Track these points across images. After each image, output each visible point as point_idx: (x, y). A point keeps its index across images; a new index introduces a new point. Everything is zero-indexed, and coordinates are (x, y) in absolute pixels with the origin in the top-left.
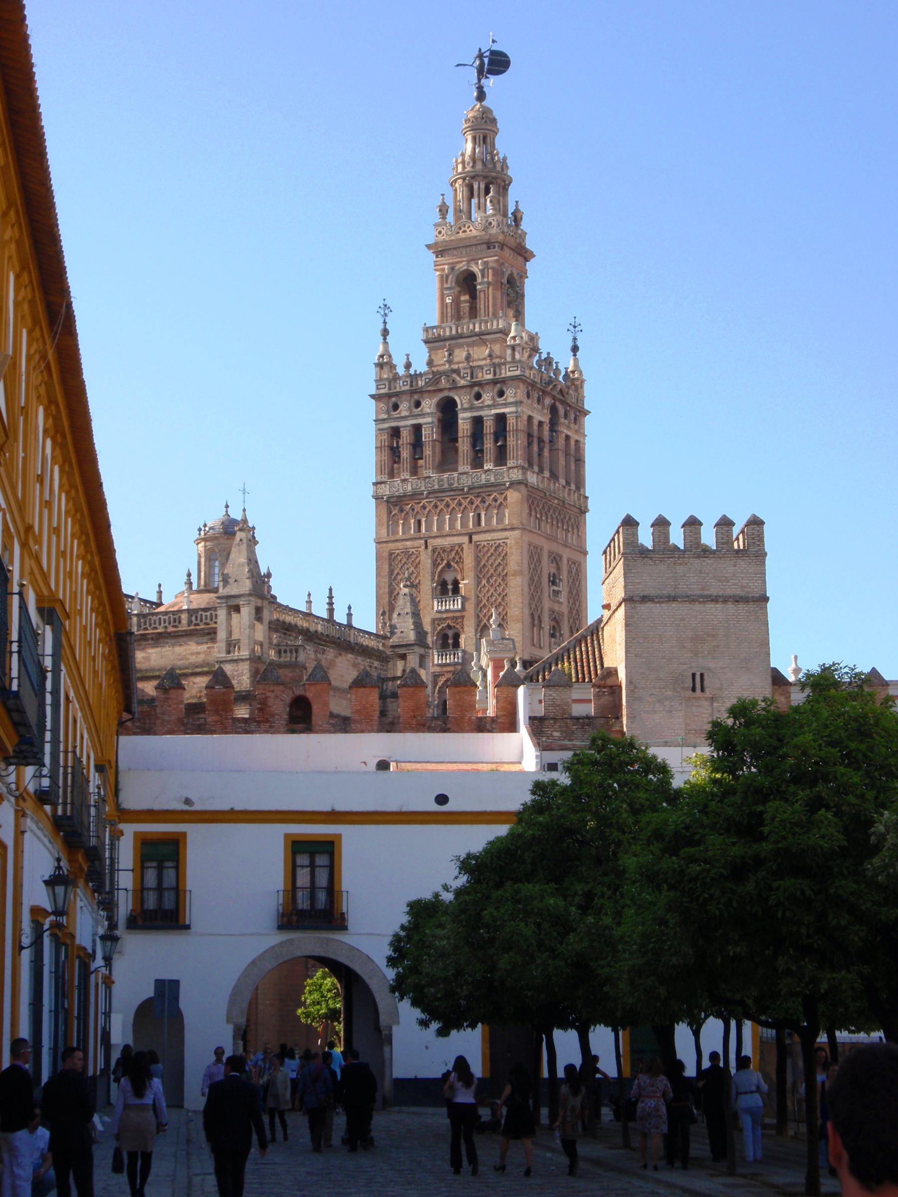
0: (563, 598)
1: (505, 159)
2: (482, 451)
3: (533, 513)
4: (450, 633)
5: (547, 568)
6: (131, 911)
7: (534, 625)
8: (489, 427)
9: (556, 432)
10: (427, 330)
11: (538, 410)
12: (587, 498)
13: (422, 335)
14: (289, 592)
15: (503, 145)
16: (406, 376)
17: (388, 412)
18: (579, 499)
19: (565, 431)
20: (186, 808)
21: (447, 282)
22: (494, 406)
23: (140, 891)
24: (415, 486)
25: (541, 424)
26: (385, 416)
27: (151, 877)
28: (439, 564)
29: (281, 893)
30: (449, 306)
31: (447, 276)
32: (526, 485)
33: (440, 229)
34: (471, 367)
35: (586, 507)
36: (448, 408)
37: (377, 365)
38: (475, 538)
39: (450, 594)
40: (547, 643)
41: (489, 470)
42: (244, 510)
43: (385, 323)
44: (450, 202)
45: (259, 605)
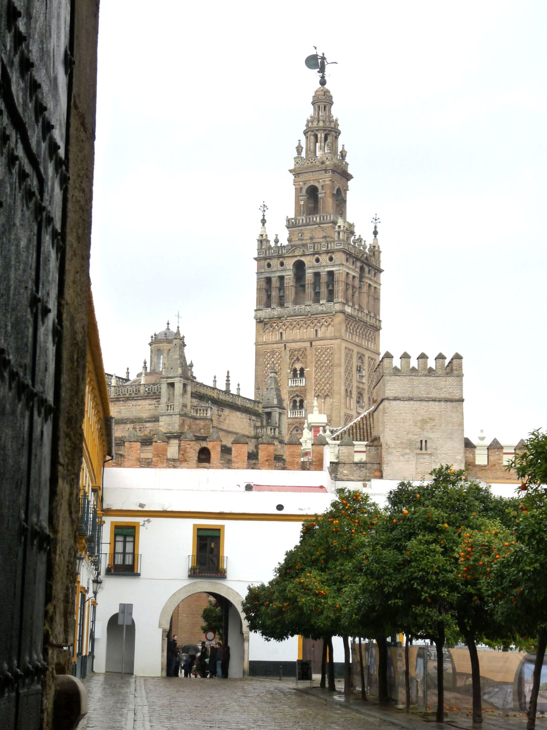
1: (337, 120)
2: (319, 292)
3: (348, 330)
4: (298, 399)
5: (355, 362)
6: (109, 565)
7: (347, 396)
8: (324, 278)
10: (288, 220)
11: (353, 270)
12: (380, 321)
13: (285, 223)
14: (203, 375)
15: (336, 111)
17: (264, 269)
18: (376, 322)
19: (369, 281)
20: (140, 509)
21: (301, 192)
22: (327, 266)
23: (114, 554)
24: (279, 312)
25: (354, 277)
26: (263, 271)
27: (119, 547)
28: (292, 359)
29: (191, 557)
31: (301, 189)
32: (344, 313)
34: (314, 243)
35: (380, 327)
36: (300, 267)
37: (258, 240)
38: (314, 343)
39: (299, 376)
40: (355, 407)
41: (323, 304)
42: (178, 327)
43: (264, 216)
44: (303, 144)
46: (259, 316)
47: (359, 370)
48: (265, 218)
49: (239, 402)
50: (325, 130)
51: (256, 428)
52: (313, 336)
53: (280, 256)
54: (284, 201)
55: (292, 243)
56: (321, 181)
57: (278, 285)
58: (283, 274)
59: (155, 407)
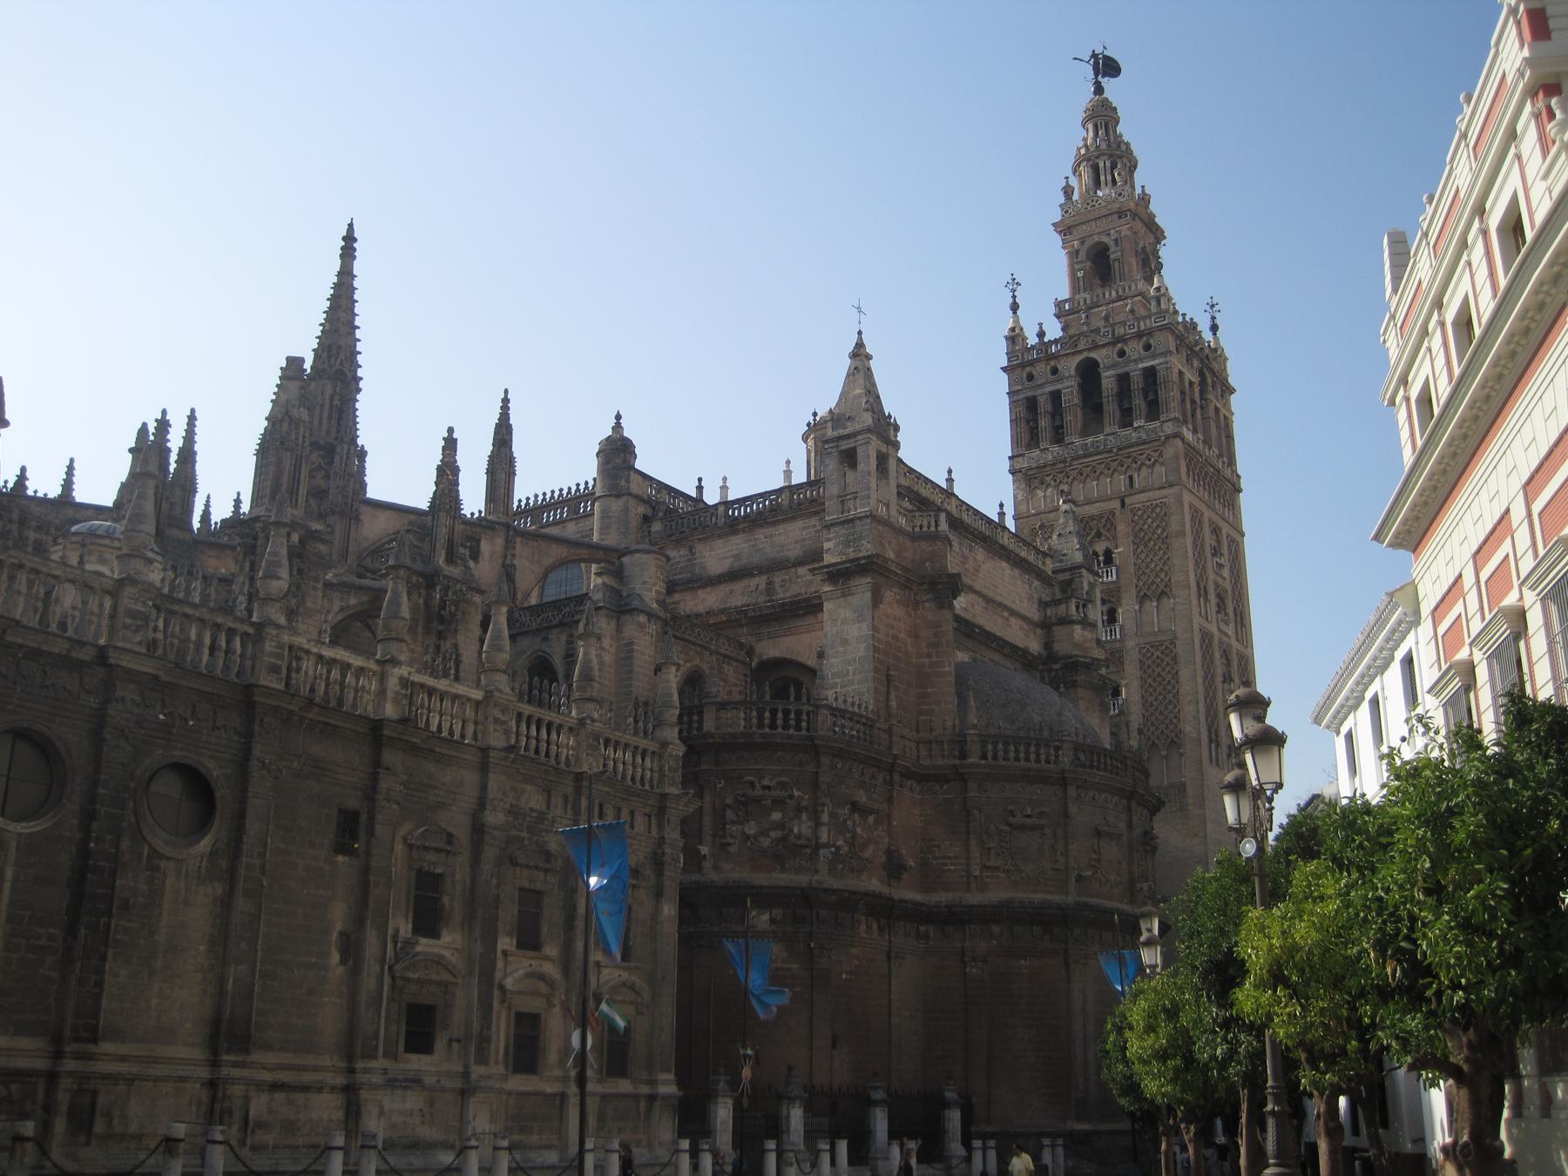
0: (1226, 573)
2: (1130, 410)
10: (1059, 304)
13: (1053, 310)
22: (1141, 360)
25: (1191, 383)
31: (1077, 252)
32: (1183, 440)
37: (1007, 338)
38: (1127, 501)
42: (860, 333)
45: (884, 450)
46: (1018, 466)
47: (1216, 552)
49: (1005, 540)
50: (1111, 156)
51: (1043, 605)
53: (1050, 357)
55: (1071, 332)
57: (1049, 408)
58: (1059, 386)
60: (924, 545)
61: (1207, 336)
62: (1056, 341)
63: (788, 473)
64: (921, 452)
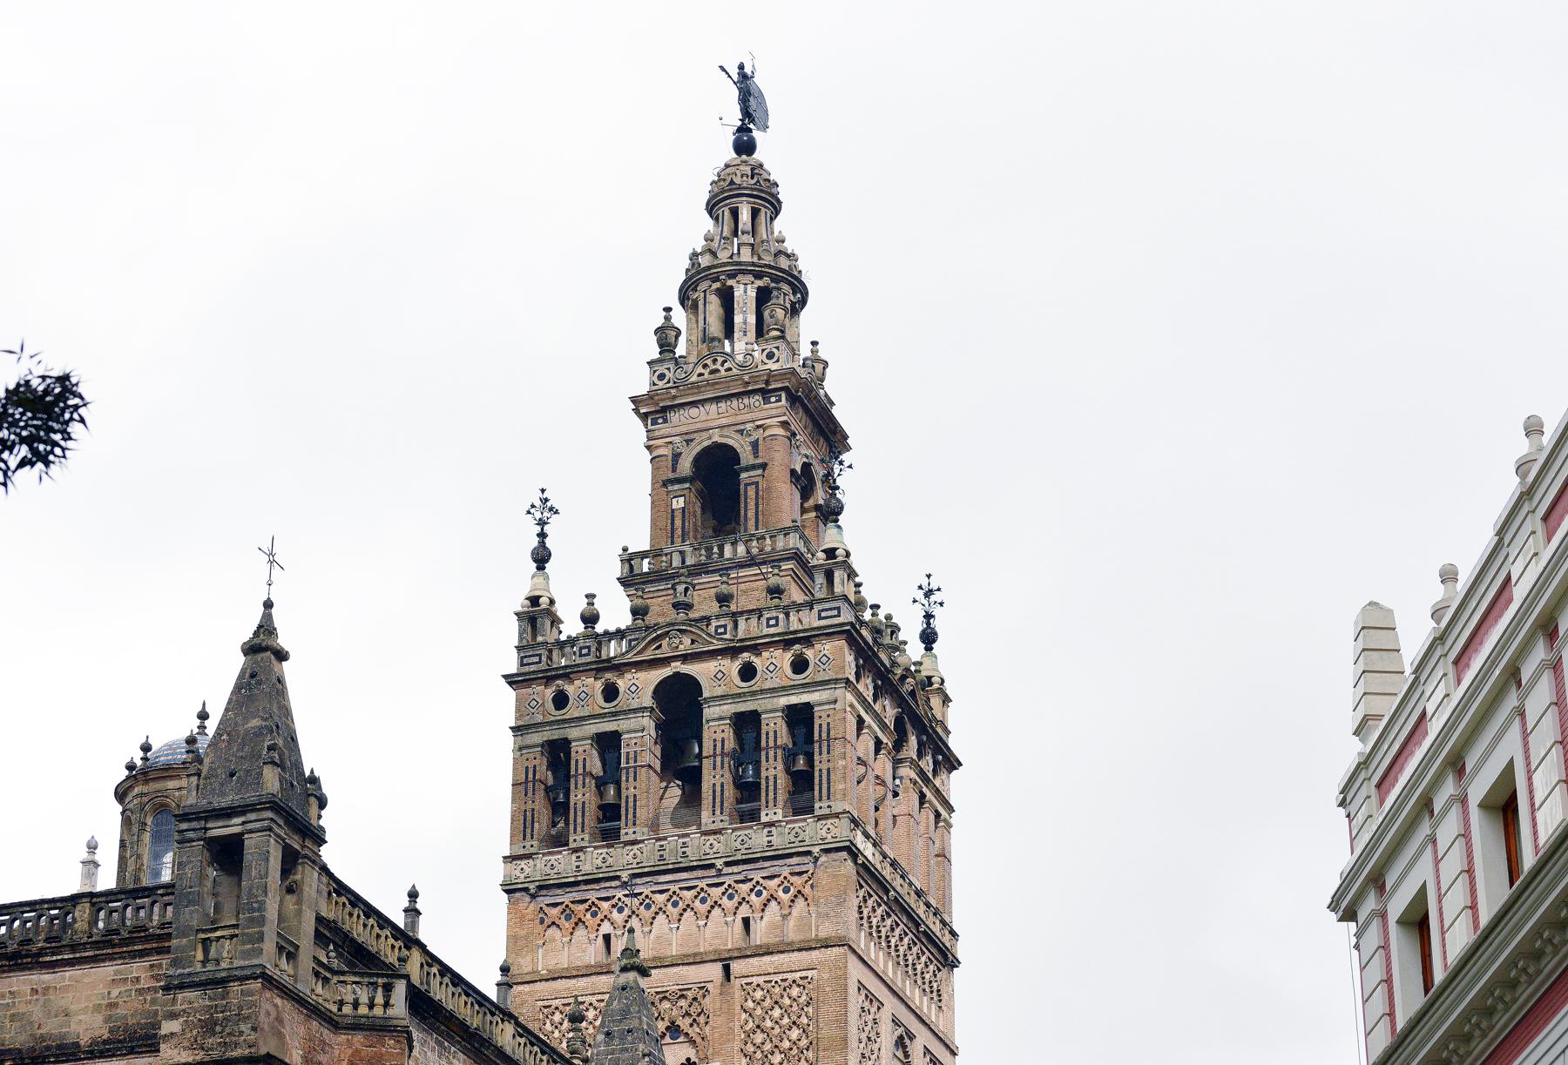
2: (756, 786)
9: (901, 778)
10: (629, 559)
12: (953, 934)
13: (617, 569)
16: (586, 637)
21: (674, 470)
24: (599, 862)
30: (678, 516)
31: (676, 457)
33: (661, 369)
34: (735, 616)
38: (736, 967)
41: (771, 824)
42: (268, 605)
43: (542, 535)
48: (549, 542)
50: (758, 276)
52: (732, 937)
53: (605, 666)
54: (613, 507)
56: (749, 426)
59: (140, 992)
60: (358, 1039)
61: (915, 650)
62: (620, 634)
63: (91, 865)
64: (365, 850)
